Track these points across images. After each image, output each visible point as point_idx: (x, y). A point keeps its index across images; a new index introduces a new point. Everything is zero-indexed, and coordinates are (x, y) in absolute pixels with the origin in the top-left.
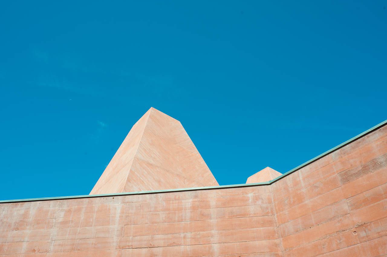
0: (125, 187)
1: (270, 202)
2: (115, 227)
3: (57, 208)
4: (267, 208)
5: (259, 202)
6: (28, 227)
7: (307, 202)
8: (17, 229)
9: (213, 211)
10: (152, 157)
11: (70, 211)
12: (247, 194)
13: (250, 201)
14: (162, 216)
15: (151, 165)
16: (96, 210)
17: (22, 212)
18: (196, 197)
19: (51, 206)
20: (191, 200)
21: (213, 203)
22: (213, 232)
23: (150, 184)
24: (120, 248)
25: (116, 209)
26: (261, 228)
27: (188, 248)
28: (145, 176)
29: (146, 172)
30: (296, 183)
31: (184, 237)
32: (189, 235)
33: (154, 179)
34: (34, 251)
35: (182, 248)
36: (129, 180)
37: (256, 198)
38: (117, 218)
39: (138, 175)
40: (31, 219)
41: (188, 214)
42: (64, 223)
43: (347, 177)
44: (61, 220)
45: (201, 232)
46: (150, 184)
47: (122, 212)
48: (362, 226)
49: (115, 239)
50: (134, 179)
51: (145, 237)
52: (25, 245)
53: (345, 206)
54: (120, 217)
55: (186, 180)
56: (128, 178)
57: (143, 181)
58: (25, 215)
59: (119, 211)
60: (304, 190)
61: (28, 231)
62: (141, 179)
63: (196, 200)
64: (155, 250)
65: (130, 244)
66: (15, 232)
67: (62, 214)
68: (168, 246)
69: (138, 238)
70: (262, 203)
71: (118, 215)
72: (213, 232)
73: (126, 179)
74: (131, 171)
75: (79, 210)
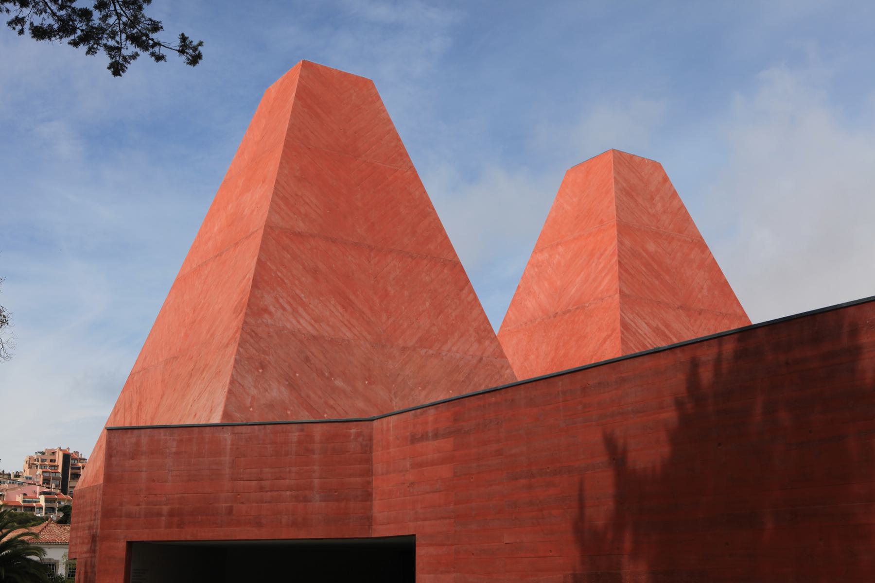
0: (249, 300)
2: (227, 459)
3: (168, 437)
5: (360, 439)
7: (391, 450)
11: (181, 441)
12: (350, 429)
13: (352, 437)
15: (300, 235)
17: (134, 440)
18: (302, 430)
19: (162, 435)
20: (297, 434)
21: (317, 437)
22: (316, 468)
23: (297, 282)
25: (226, 440)
26: (358, 466)
28: (286, 267)
29: (289, 256)
31: (290, 472)
32: (294, 469)
33: (304, 268)
34: (154, 481)
35: (288, 481)
36: (255, 285)
37: (358, 435)
38: (228, 450)
39: (274, 268)
40: (144, 449)
42: (177, 453)
43: (414, 439)
44: (174, 450)
45: (305, 468)
46: (297, 282)
47: (232, 445)
48: (412, 484)
50: (266, 278)
52: (144, 475)
54: (231, 449)
55: (372, 254)
56: (253, 280)
57: (282, 280)
58: (138, 444)
59: (229, 442)
60: (391, 438)
61: (144, 461)
62: (279, 274)
63: (302, 433)
64: (264, 483)
65: (241, 476)
66: (131, 461)
67: (175, 444)
68: (276, 479)
69: (248, 470)
71: (228, 447)
72: (316, 468)
73: (251, 281)
74: (259, 261)
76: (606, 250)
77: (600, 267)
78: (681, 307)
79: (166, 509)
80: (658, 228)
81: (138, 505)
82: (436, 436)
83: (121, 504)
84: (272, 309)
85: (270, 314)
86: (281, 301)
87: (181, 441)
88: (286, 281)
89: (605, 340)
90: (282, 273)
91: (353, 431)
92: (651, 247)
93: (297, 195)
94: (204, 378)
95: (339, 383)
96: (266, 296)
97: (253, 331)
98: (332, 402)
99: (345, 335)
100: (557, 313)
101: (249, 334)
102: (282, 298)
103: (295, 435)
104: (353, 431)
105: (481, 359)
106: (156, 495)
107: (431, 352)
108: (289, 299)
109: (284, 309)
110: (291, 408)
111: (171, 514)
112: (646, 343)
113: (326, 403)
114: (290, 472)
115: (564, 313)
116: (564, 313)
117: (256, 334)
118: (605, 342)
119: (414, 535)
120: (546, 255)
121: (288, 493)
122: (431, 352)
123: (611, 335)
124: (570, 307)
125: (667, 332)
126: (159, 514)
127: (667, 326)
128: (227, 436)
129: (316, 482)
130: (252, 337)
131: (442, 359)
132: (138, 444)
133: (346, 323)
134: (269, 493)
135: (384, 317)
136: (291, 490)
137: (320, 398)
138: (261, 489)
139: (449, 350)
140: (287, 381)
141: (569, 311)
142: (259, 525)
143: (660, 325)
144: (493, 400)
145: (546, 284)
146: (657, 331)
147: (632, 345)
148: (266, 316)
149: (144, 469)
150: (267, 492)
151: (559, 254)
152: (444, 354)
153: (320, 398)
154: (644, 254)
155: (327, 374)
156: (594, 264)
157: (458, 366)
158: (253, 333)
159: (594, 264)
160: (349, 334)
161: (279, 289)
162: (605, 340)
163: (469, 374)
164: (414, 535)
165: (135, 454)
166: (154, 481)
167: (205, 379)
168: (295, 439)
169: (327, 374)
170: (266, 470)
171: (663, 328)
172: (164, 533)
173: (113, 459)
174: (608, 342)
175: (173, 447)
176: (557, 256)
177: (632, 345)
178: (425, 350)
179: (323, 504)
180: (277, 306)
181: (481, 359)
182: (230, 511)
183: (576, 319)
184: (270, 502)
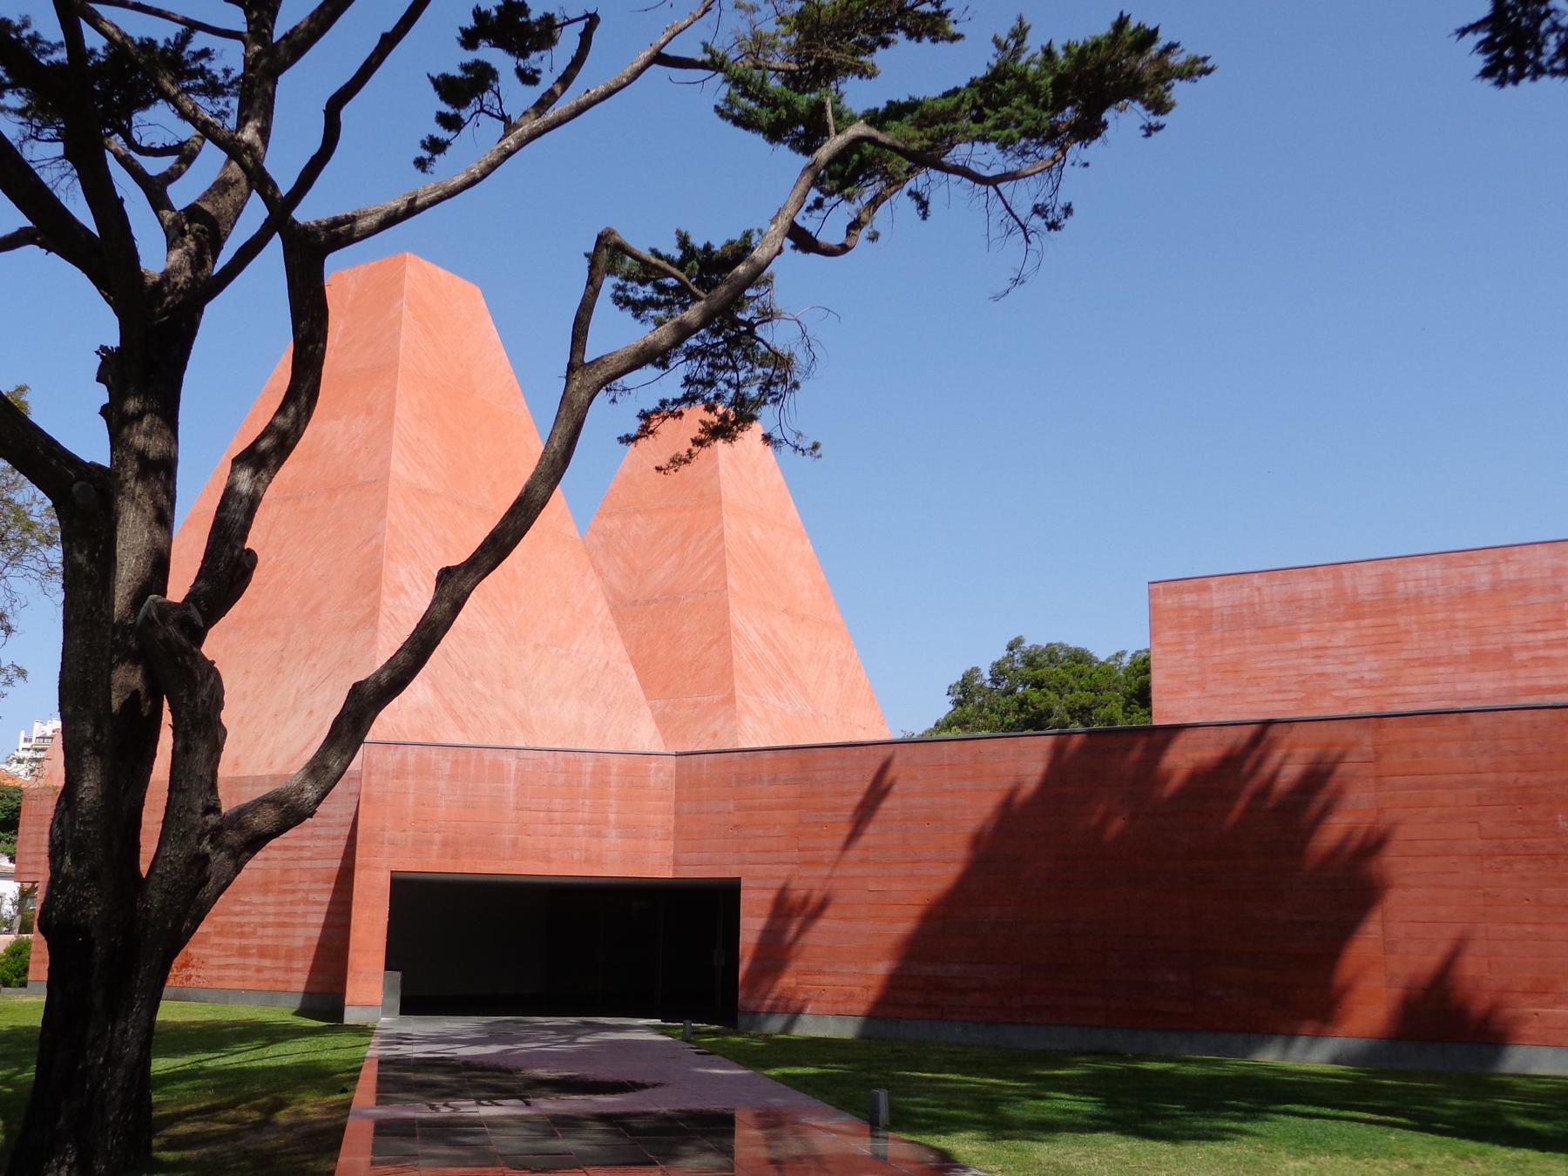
1: (671, 776)
2: (511, 786)
4: (668, 782)
5: (661, 774)
6: (410, 777)
8: (397, 778)
9: (613, 779)
10: (424, 463)
12: (650, 763)
13: (653, 771)
14: (561, 778)
16: (487, 763)
17: (398, 756)
20: (591, 764)
21: (614, 770)
22: (612, 801)
24: (517, 809)
27: (586, 816)
30: (700, 766)
31: (583, 804)
32: (587, 802)
33: (434, 536)
35: (580, 814)
37: (659, 770)
38: (512, 776)
39: (405, 534)
41: (587, 780)
42: (449, 775)
46: (428, 554)
47: (518, 770)
49: (512, 799)
50: (398, 547)
51: (544, 800)
52: (411, 798)
53: (731, 807)
54: (516, 775)
58: (403, 762)
59: (513, 768)
61: (411, 782)
63: (597, 764)
65: (528, 806)
66: (395, 781)
67: (448, 765)
68: (568, 811)
70: (664, 775)
71: (513, 773)
72: (612, 801)
75: (468, 762)
76: (708, 531)
77: (701, 552)
78: (785, 611)
79: (438, 837)
80: (761, 509)
81: (404, 831)
82: (774, 780)
83: (383, 829)
84: (408, 588)
85: (406, 593)
86: (416, 577)
87: (455, 763)
88: (419, 553)
89: (710, 645)
90: (414, 541)
91: (653, 765)
92: (756, 533)
93: (419, 439)
94: (315, 665)
95: (478, 684)
96: (401, 570)
97: (392, 615)
98: (473, 709)
99: (480, 625)
100: (636, 601)
101: (389, 618)
102: (416, 574)
103: (589, 764)
104: (653, 765)
105: (608, 663)
106: (426, 821)
107: (561, 652)
108: (423, 576)
109: (419, 588)
110: (437, 713)
111: (445, 843)
112: (756, 652)
113: (469, 709)
114: (583, 804)
115: (648, 603)
116: (648, 603)
117: (395, 618)
118: (710, 648)
119: (740, 878)
120: (615, 523)
121: (581, 827)
122: (561, 652)
123: (719, 640)
124: (657, 596)
125: (774, 641)
126: (430, 842)
127: (774, 633)
128: (510, 761)
129: (612, 817)
130: (391, 621)
131: (572, 662)
132: (403, 762)
133: (479, 609)
134: (559, 827)
135: (515, 607)
136: (584, 825)
137: (462, 702)
138: (551, 822)
139: (578, 651)
140: (430, 679)
141: (656, 601)
142: (548, 860)
143: (769, 633)
144: (857, 753)
145: (619, 560)
146: (764, 637)
147: (743, 655)
148: (403, 596)
149: (411, 791)
150: (557, 824)
151: (637, 525)
152: (573, 654)
153: (462, 702)
154: (750, 542)
155: (466, 674)
156: (691, 547)
157: (587, 670)
158: (392, 618)
159: (691, 547)
160: (483, 624)
161: (412, 562)
162: (710, 645)
163: (597, 682)
164: (740, 878)
165: (400, 773)
166: (423, 805)
167: (318, 667)
168: (589, 769)
169: (466, 674)
170: (557, 801)
171: (769, 633)
172: (433, 862)
173: (373, 777)
174: (715, 647)
175: (447, 767)
176: (635, 527)
177: (743, 655)
178: (555, 649)
179: (620, 841)
180: (413, 584)
181: (608, 663)
182: (515, 843)
183: (667, 613)
184: (560, 836)
